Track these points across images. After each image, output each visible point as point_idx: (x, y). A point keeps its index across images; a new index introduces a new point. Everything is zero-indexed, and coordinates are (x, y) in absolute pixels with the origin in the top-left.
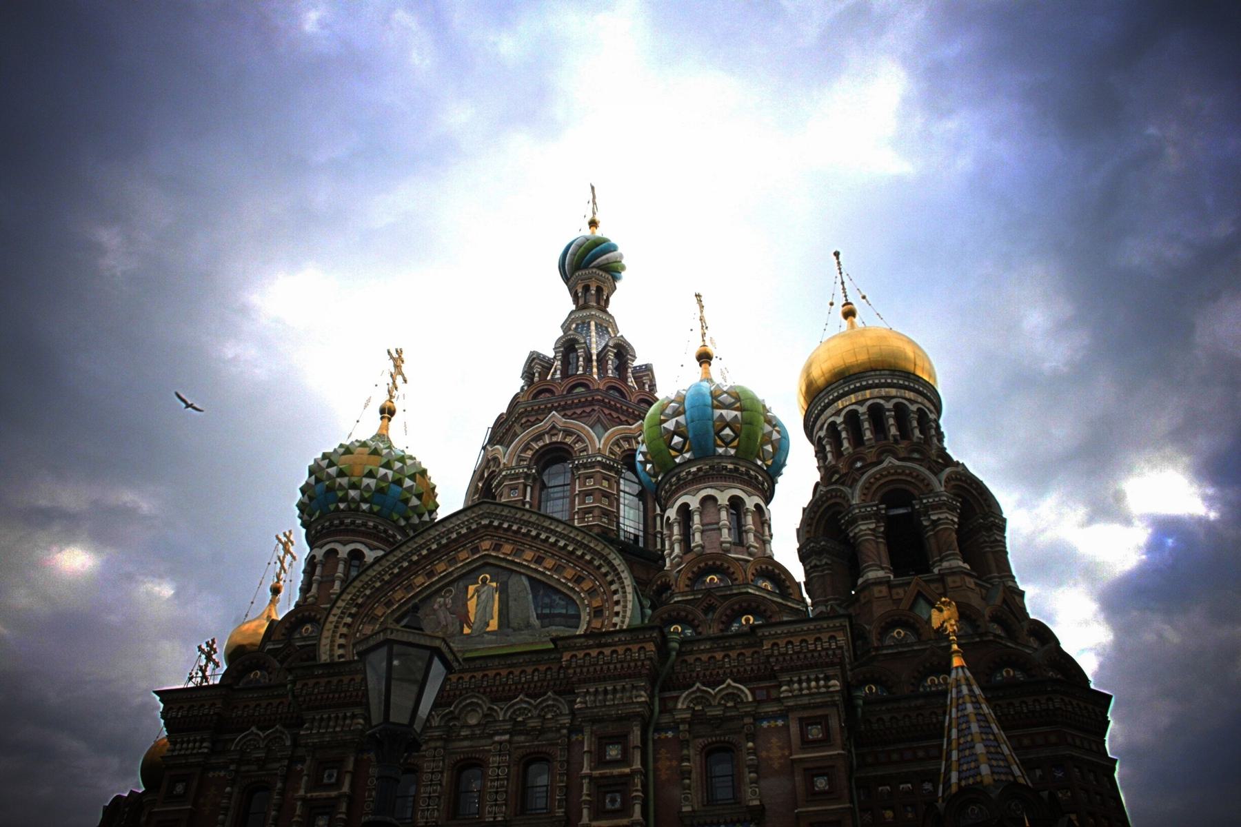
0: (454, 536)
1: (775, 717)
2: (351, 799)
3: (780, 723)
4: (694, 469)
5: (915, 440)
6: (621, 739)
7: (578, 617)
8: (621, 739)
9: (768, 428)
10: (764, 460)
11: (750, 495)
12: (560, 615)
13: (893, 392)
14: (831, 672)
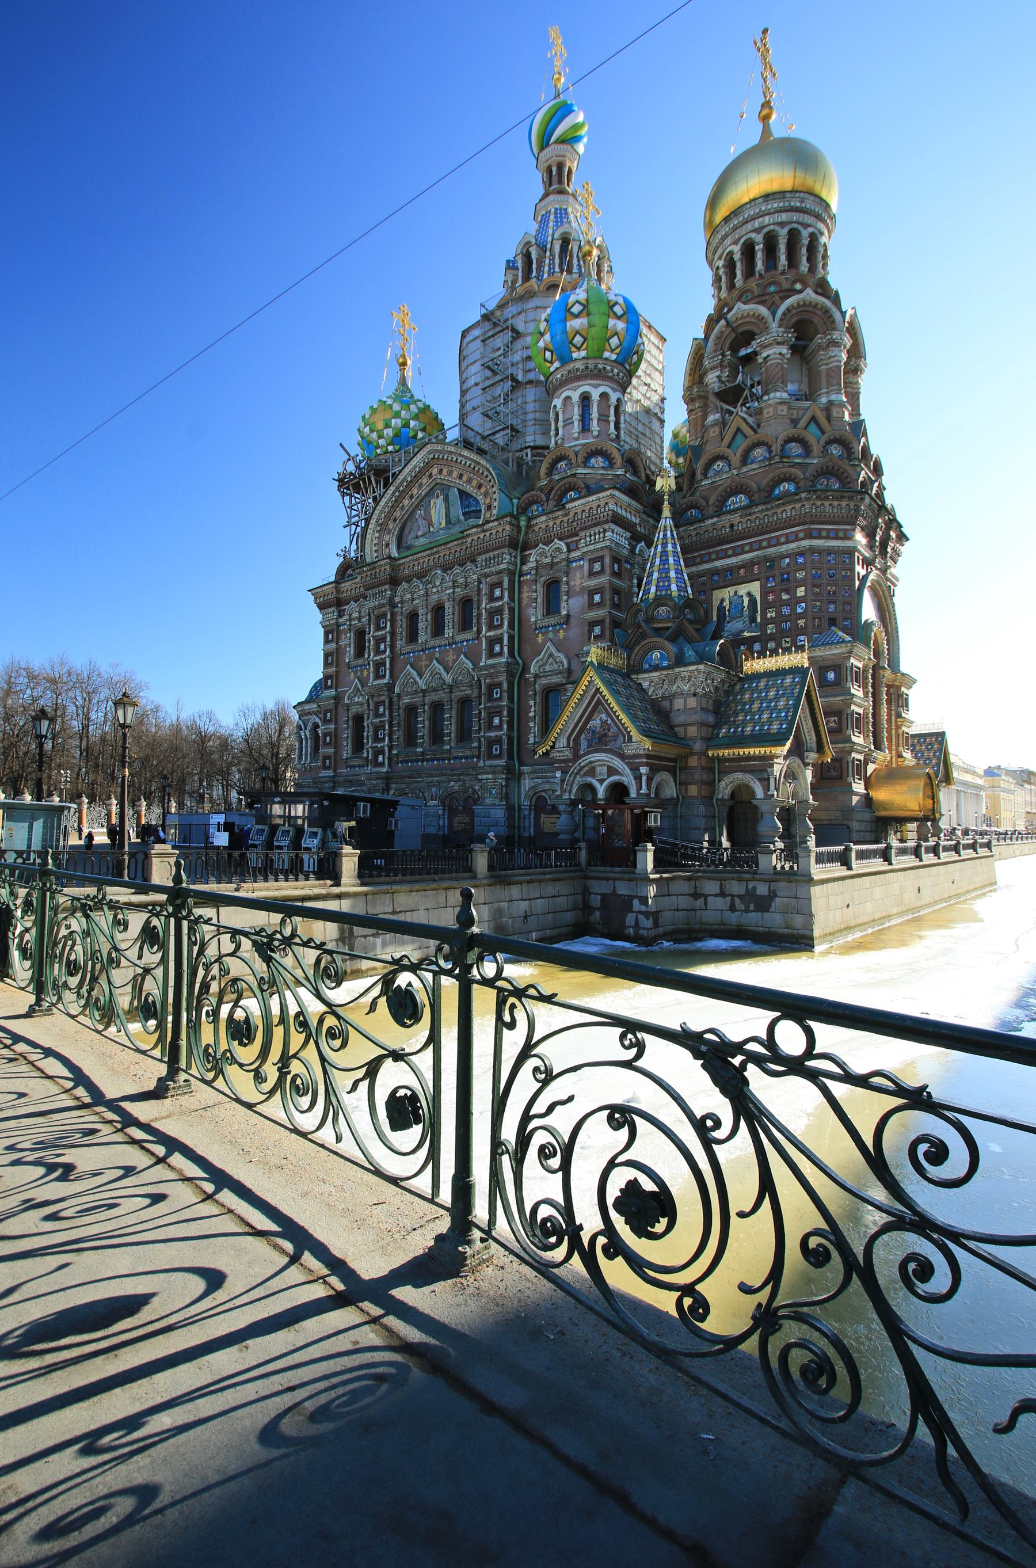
0: (417, 469)
1: (579, 560)
2: (393, 634)
3: (582, 563)
4: (559, 376)
5: (781, 268)
6: (500, 584)
7: (480, 511)
8: (500, 584)
9: (612, 322)
10: (612, 351)
11: (596, 387)
12: (473, 511)
13: (767, 218)
14: (606, 526)
